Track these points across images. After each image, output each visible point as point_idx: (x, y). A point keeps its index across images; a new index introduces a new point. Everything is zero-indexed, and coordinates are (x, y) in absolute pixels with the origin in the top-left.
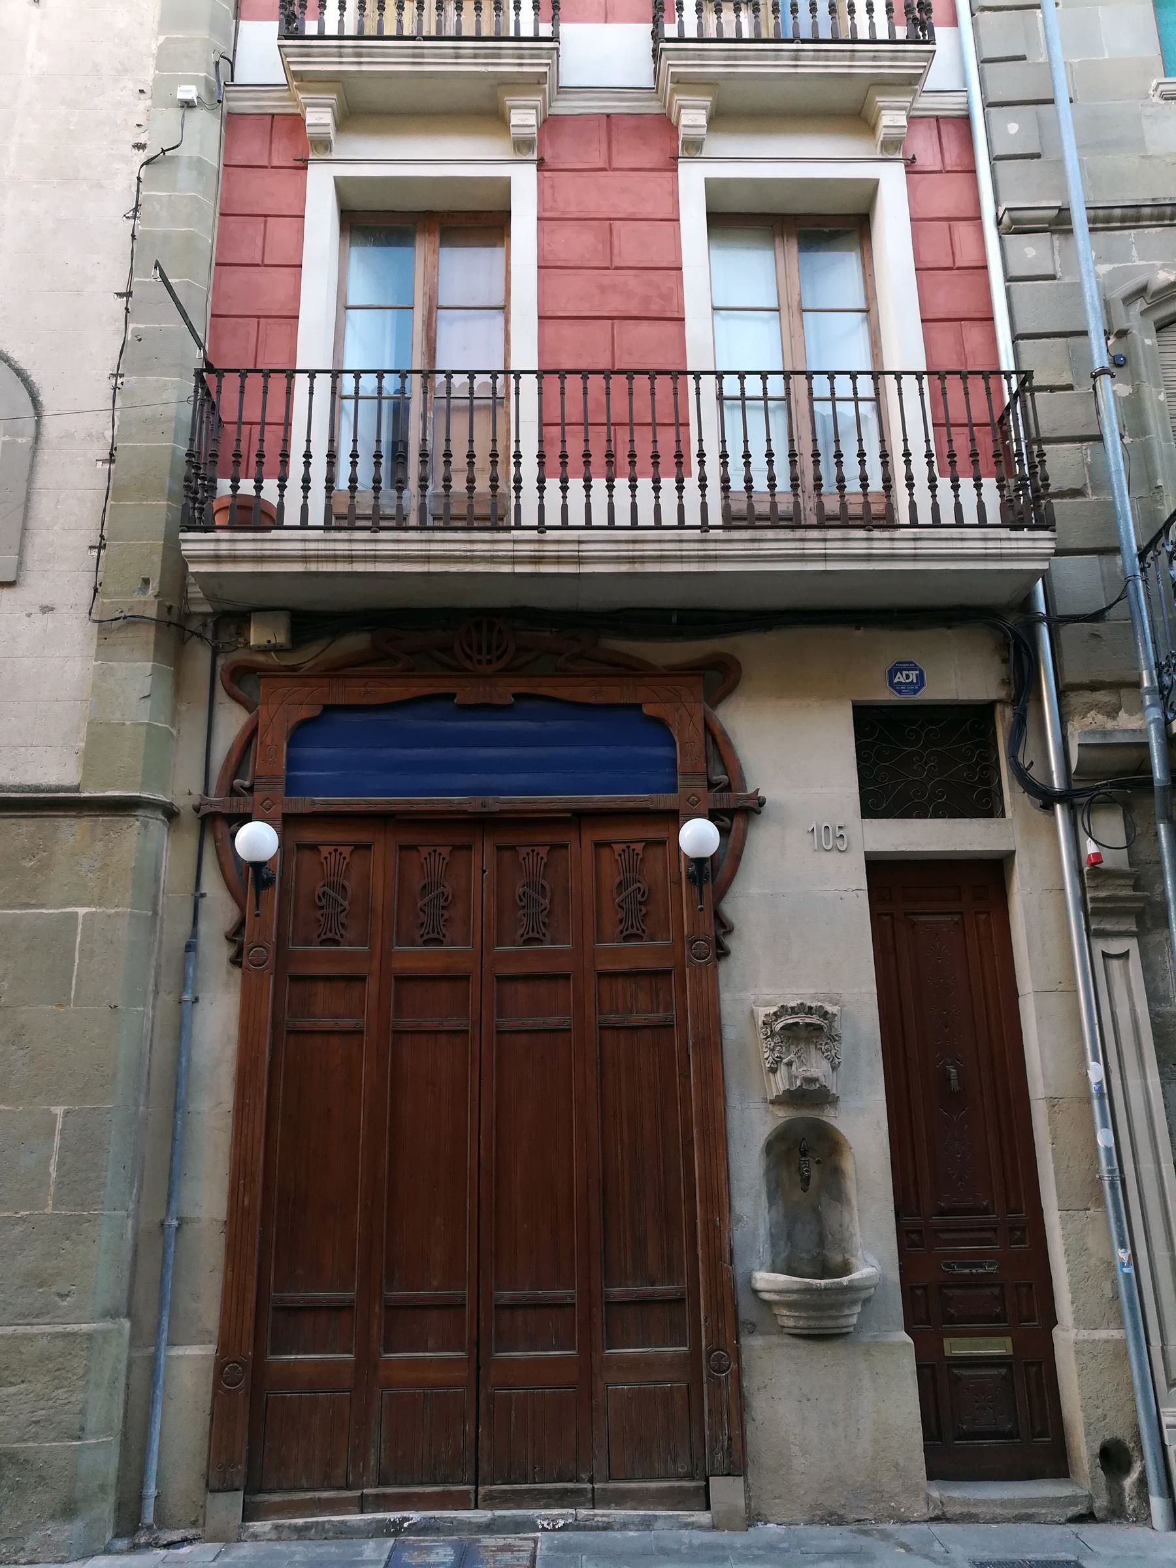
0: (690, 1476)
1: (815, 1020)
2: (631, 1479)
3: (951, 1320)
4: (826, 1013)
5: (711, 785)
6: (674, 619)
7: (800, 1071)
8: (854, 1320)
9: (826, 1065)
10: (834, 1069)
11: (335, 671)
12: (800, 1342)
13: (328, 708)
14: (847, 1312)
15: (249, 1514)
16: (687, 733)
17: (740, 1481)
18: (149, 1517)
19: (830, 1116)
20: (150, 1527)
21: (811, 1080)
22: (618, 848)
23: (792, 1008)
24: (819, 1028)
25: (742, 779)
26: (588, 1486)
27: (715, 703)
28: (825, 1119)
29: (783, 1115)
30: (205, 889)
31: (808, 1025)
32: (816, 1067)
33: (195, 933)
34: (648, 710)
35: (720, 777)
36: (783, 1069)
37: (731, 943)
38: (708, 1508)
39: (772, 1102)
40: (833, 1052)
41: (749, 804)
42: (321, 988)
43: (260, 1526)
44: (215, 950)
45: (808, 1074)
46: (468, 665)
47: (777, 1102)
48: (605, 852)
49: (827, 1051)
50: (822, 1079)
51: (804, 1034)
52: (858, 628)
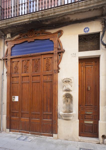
0: (51, 133)
1: (69, 80)
2: (45, 133)
3: (86, 119)
5: (58, 49)
6: (54, 26)
7: (67, 87)
8: (72, 118)
9: (70, 86)
11: (15, 40)
12: (65, 120)
13: (15, 45)
14: (70, 117)
15: (10, 131)
16: (55, 42)
17: (57, 134)
18: (2, 130)
19: (70, 93)
20: (2, 131)
22: (46, 59)
24: (69, 81)
25: (62, 48)
26: (40, 133)
27: (59, 37)
28: (70, 93)
29: (65, 92)
30: (4, 68)
31: (68, 81)
32: (68, 86)
33: (3, 73)
34: (50, 39)
35: (59, 48)
36: (65, 87)
37: (60, 70)
38: (53, 137)
41: (63, 51)
42: (15, 78)
43: (11, 132)
44: (5, 74)
45: (68, 88)
46: (29, 37)
48: (45, 59)
51: (67, 82)
52: (80, 23)
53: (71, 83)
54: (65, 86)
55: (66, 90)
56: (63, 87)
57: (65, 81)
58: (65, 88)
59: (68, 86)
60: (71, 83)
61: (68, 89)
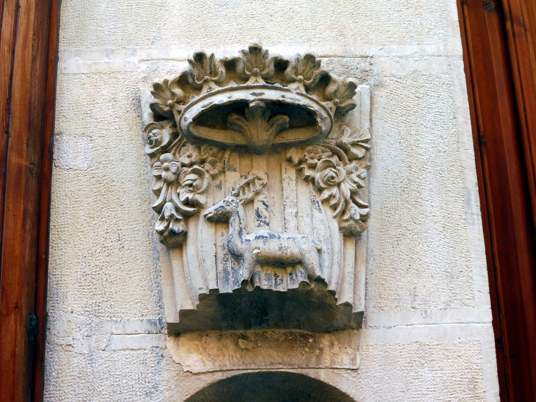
1: (294, 95)
4: (325, 79)
7: (254, 239)
10: (351, 234)
21: (282, 264)
23: (230, 65)
24: (303, 117)
28: (323, 376)
31: (276, 108)
32: (291, 222)
36: (202, 238)
39: (176, 331)
40: (347, 188)
45: (272, 248)
47: (182, 328)
49: (330, 182)
50: (312, 259)
51: (260, 133)
53: (343, 152)
54: (221, 220)
55: (232, 313)
56: (174, 241)
57: (214, 117)
58: (205, 267)
59: (291, 222)
60: (343, 152)
61: (287, 283)
